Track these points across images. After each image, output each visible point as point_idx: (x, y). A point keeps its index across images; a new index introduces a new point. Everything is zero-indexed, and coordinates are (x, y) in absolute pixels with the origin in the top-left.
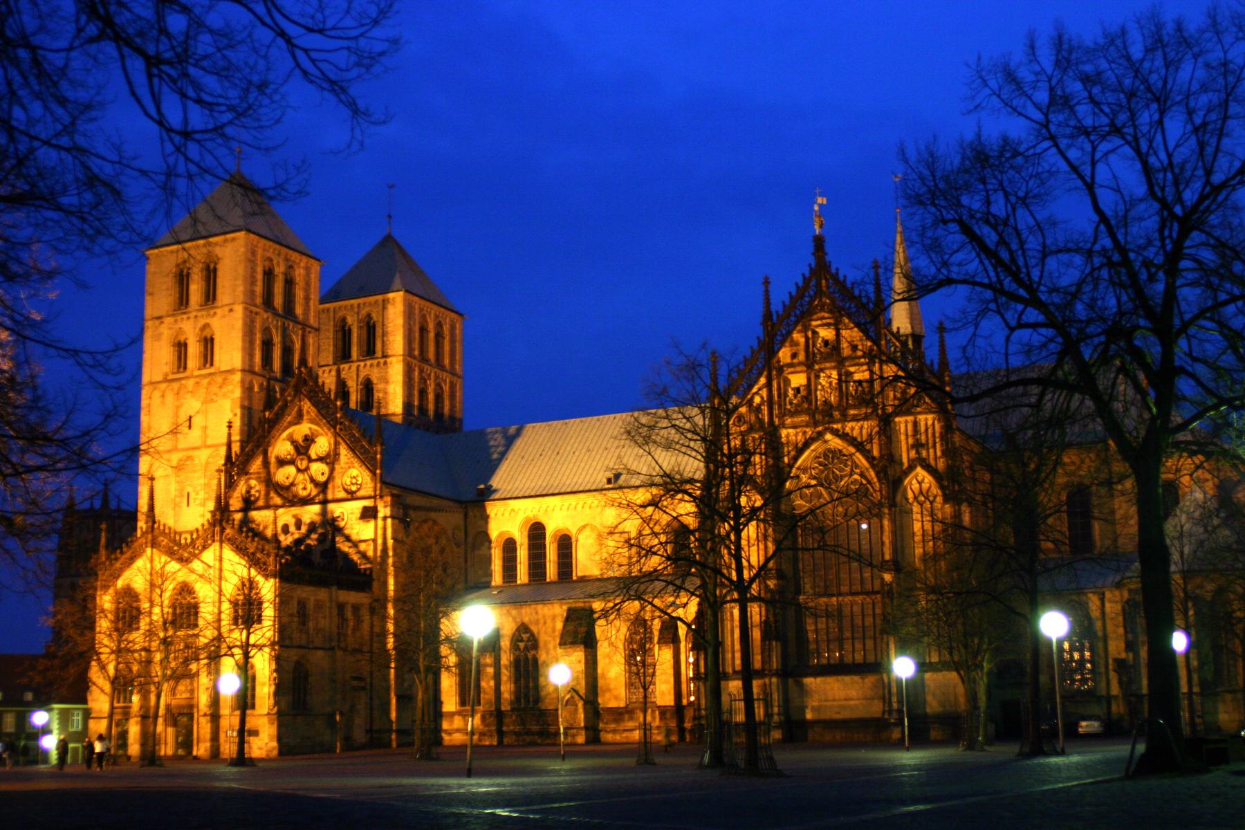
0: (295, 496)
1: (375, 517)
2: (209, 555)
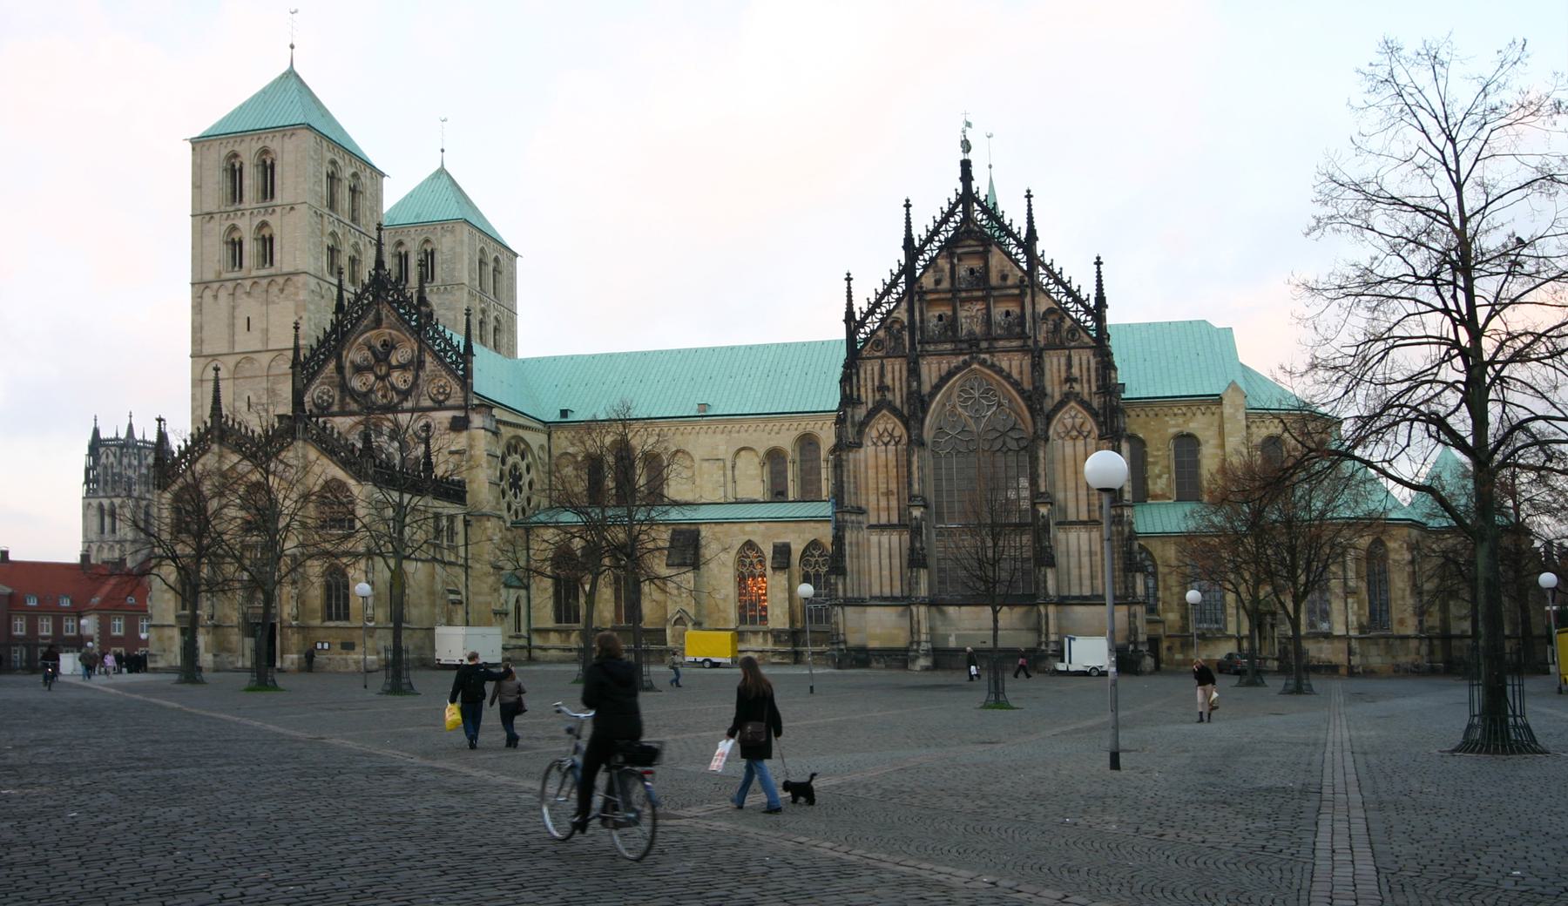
0: (374, 403)
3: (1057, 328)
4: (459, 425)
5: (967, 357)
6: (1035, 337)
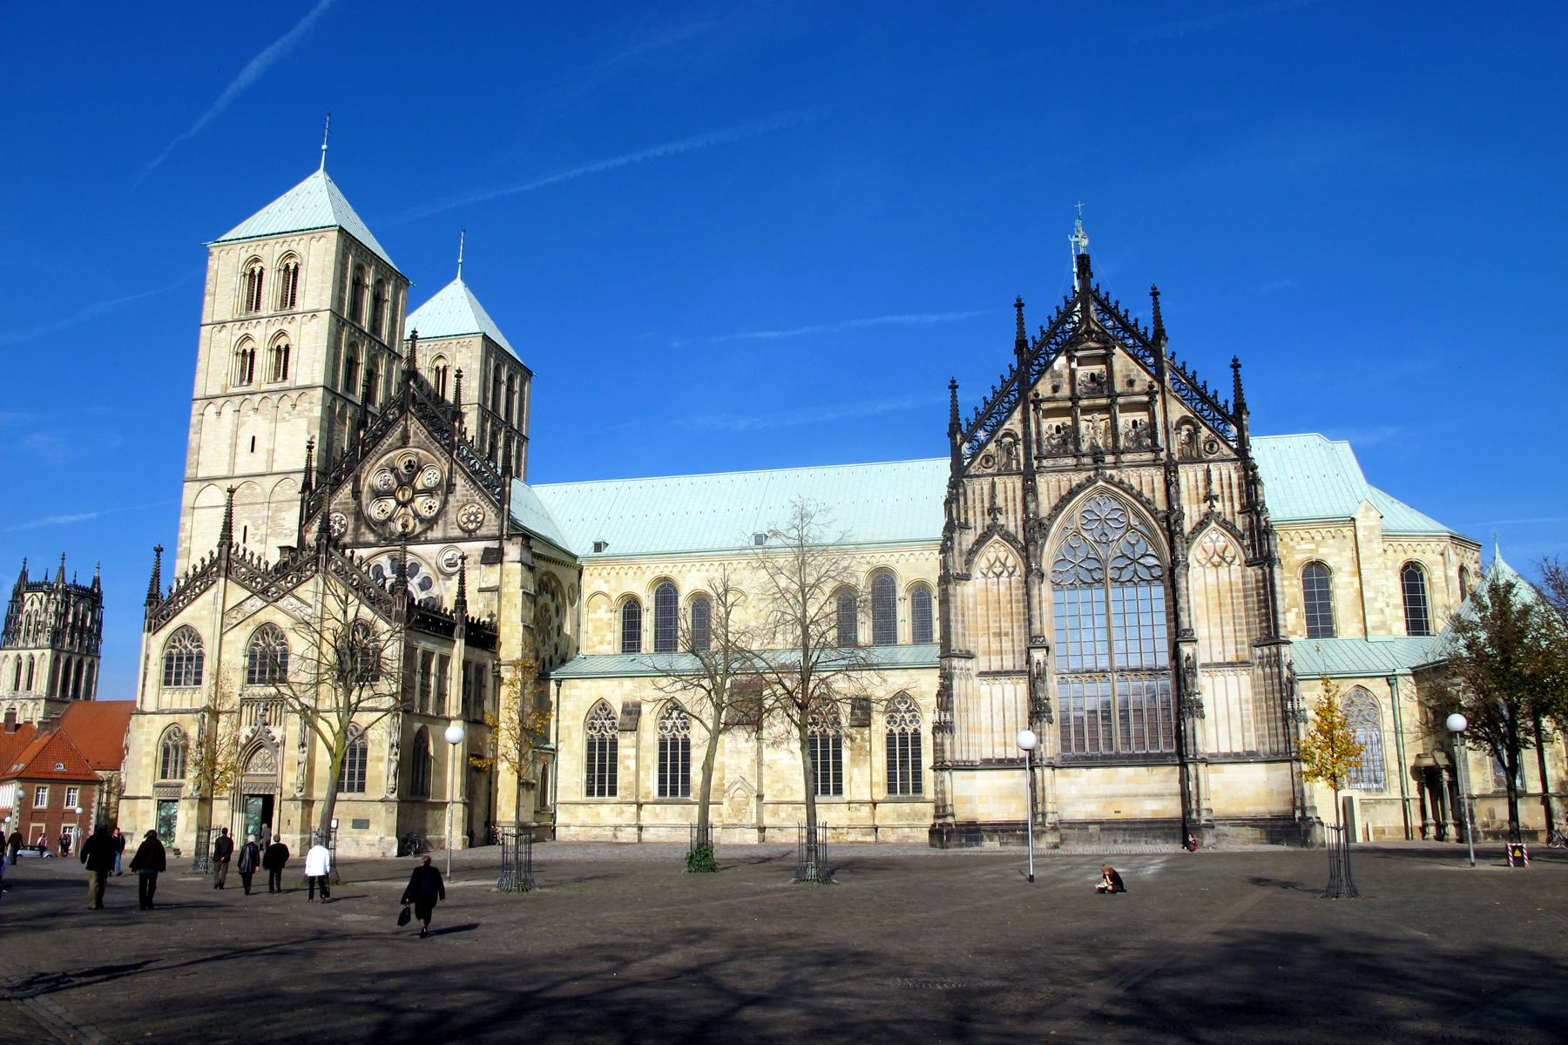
0: (392, 533)
1: (501, 562)
3: (1192, 437)
4: (493, 557)
5: (1092, 473)
6: (1169, 449)
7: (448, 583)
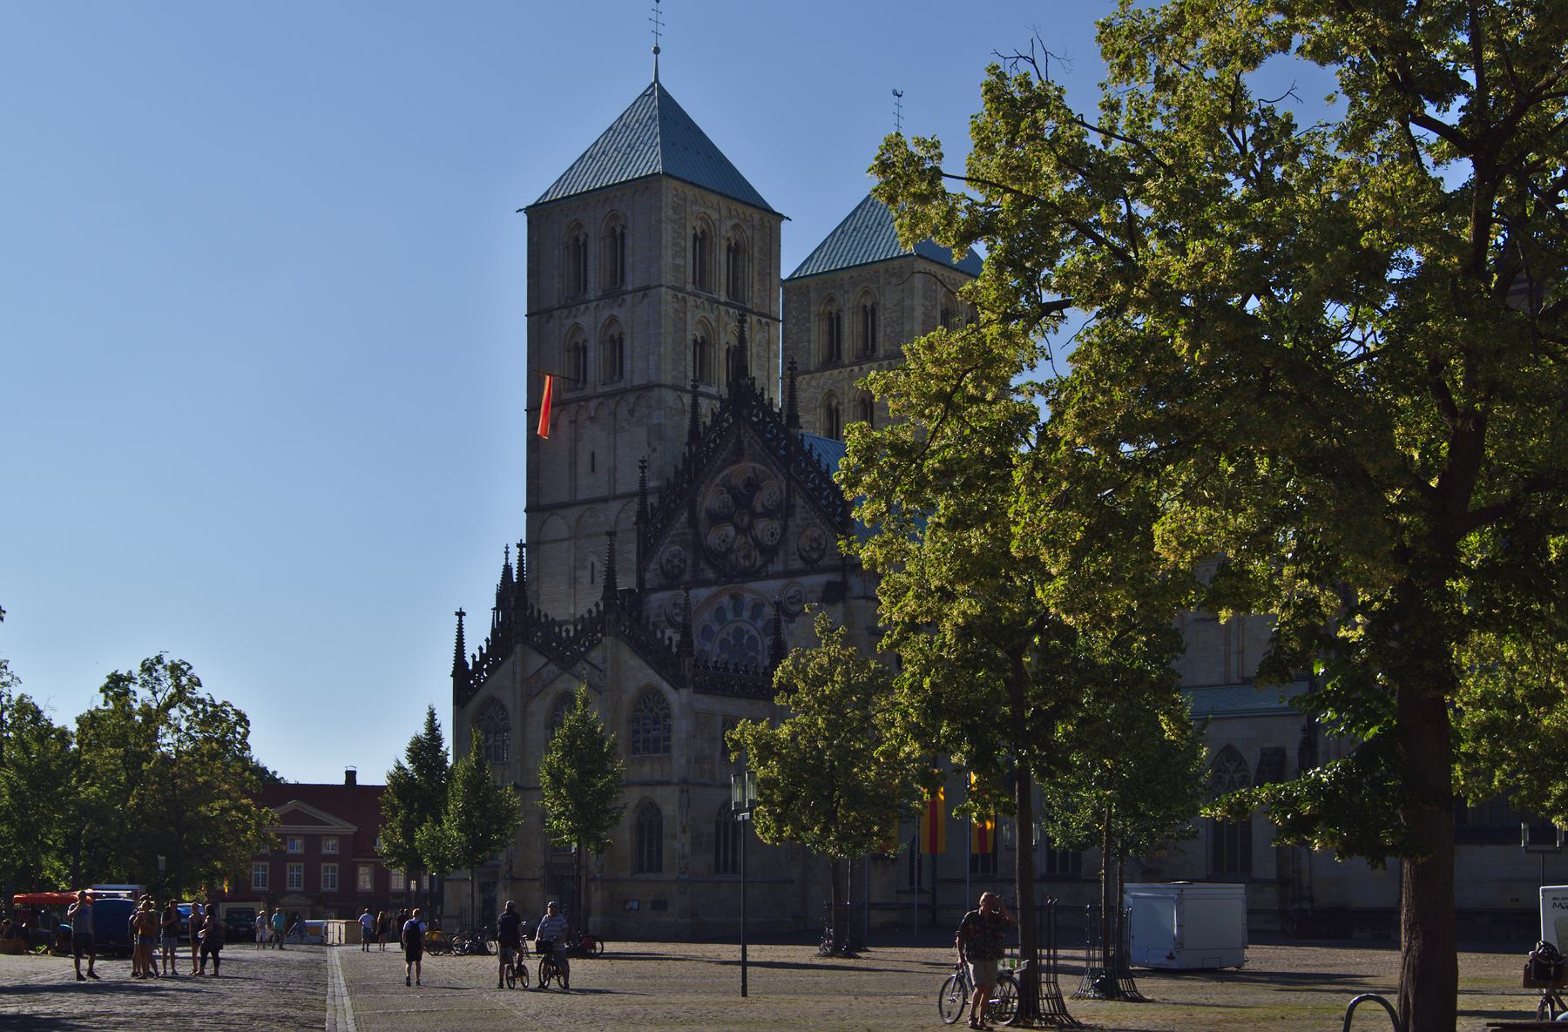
2: (595, 656)
7: (792, 626)
